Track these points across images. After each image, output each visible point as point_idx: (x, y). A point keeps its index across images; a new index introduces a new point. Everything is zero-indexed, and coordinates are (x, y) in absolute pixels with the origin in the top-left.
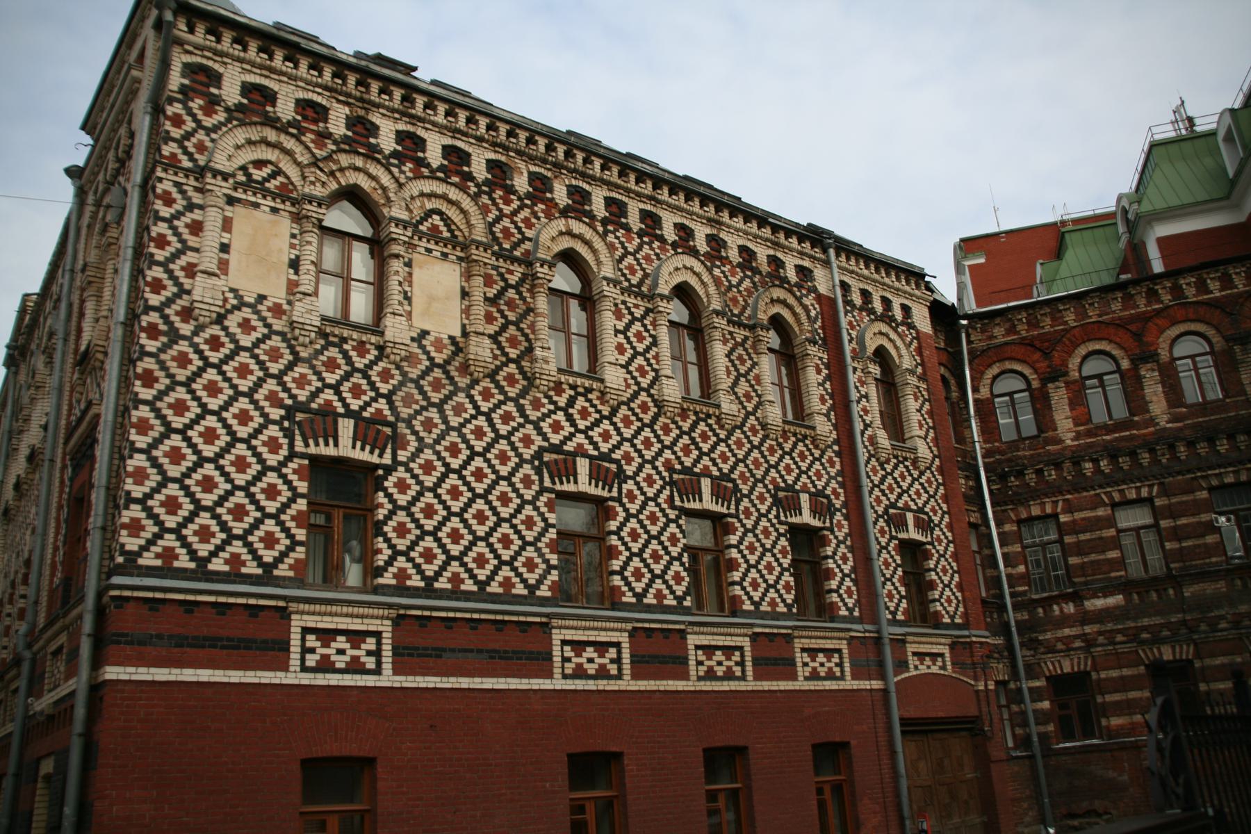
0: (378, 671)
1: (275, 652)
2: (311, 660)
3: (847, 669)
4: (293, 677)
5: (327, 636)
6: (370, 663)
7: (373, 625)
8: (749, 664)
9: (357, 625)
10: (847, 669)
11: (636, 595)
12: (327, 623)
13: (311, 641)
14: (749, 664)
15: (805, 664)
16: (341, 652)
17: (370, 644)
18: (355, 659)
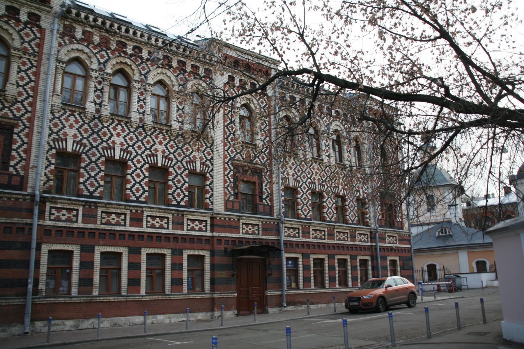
0: (258, 234)
1: (236, 229)
2: (244, 231)
3: (349, 238)
4: (241, 235)
5: (247, 225)
6: (256, 232)
7: (257, 223)
8: (326, 235)
9: (254, 223)
10: (349, 238)
11: (305, 215)
12: (247, 222)
13: (244, 226)
14: (326, 235)
15: (337, 236)
16: (250, 229)
17: (256, 227)
18: (253, 231)
